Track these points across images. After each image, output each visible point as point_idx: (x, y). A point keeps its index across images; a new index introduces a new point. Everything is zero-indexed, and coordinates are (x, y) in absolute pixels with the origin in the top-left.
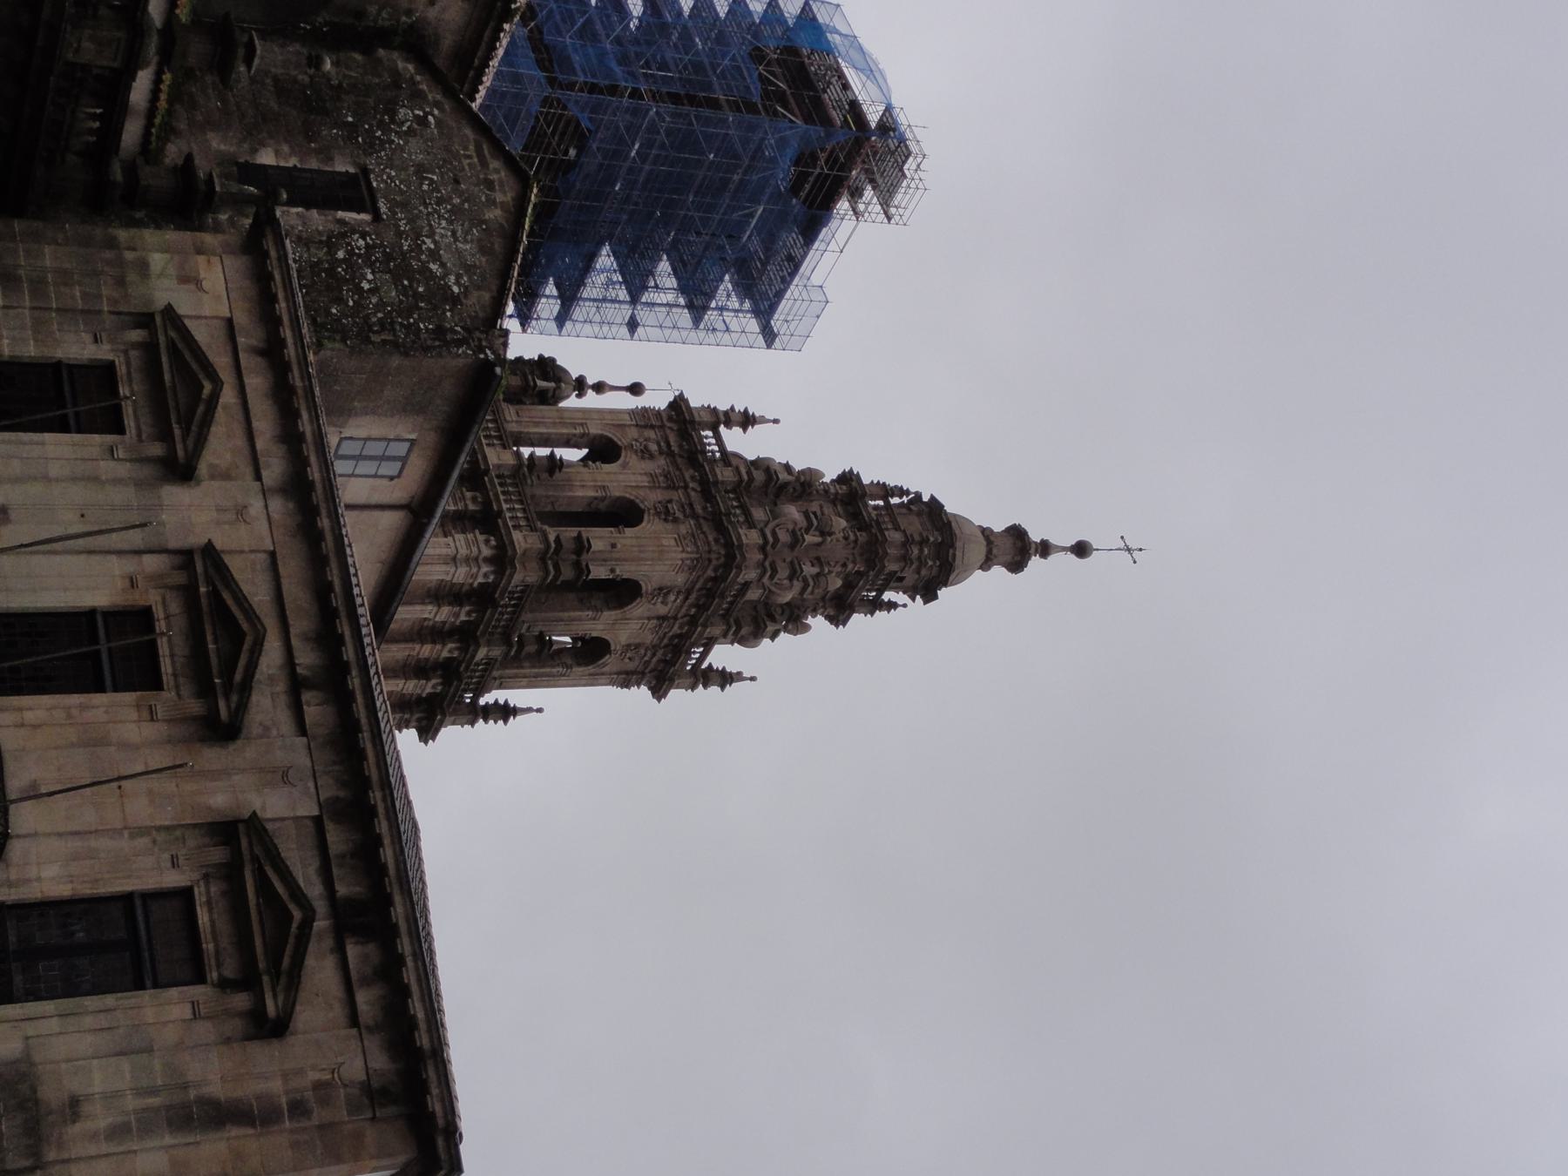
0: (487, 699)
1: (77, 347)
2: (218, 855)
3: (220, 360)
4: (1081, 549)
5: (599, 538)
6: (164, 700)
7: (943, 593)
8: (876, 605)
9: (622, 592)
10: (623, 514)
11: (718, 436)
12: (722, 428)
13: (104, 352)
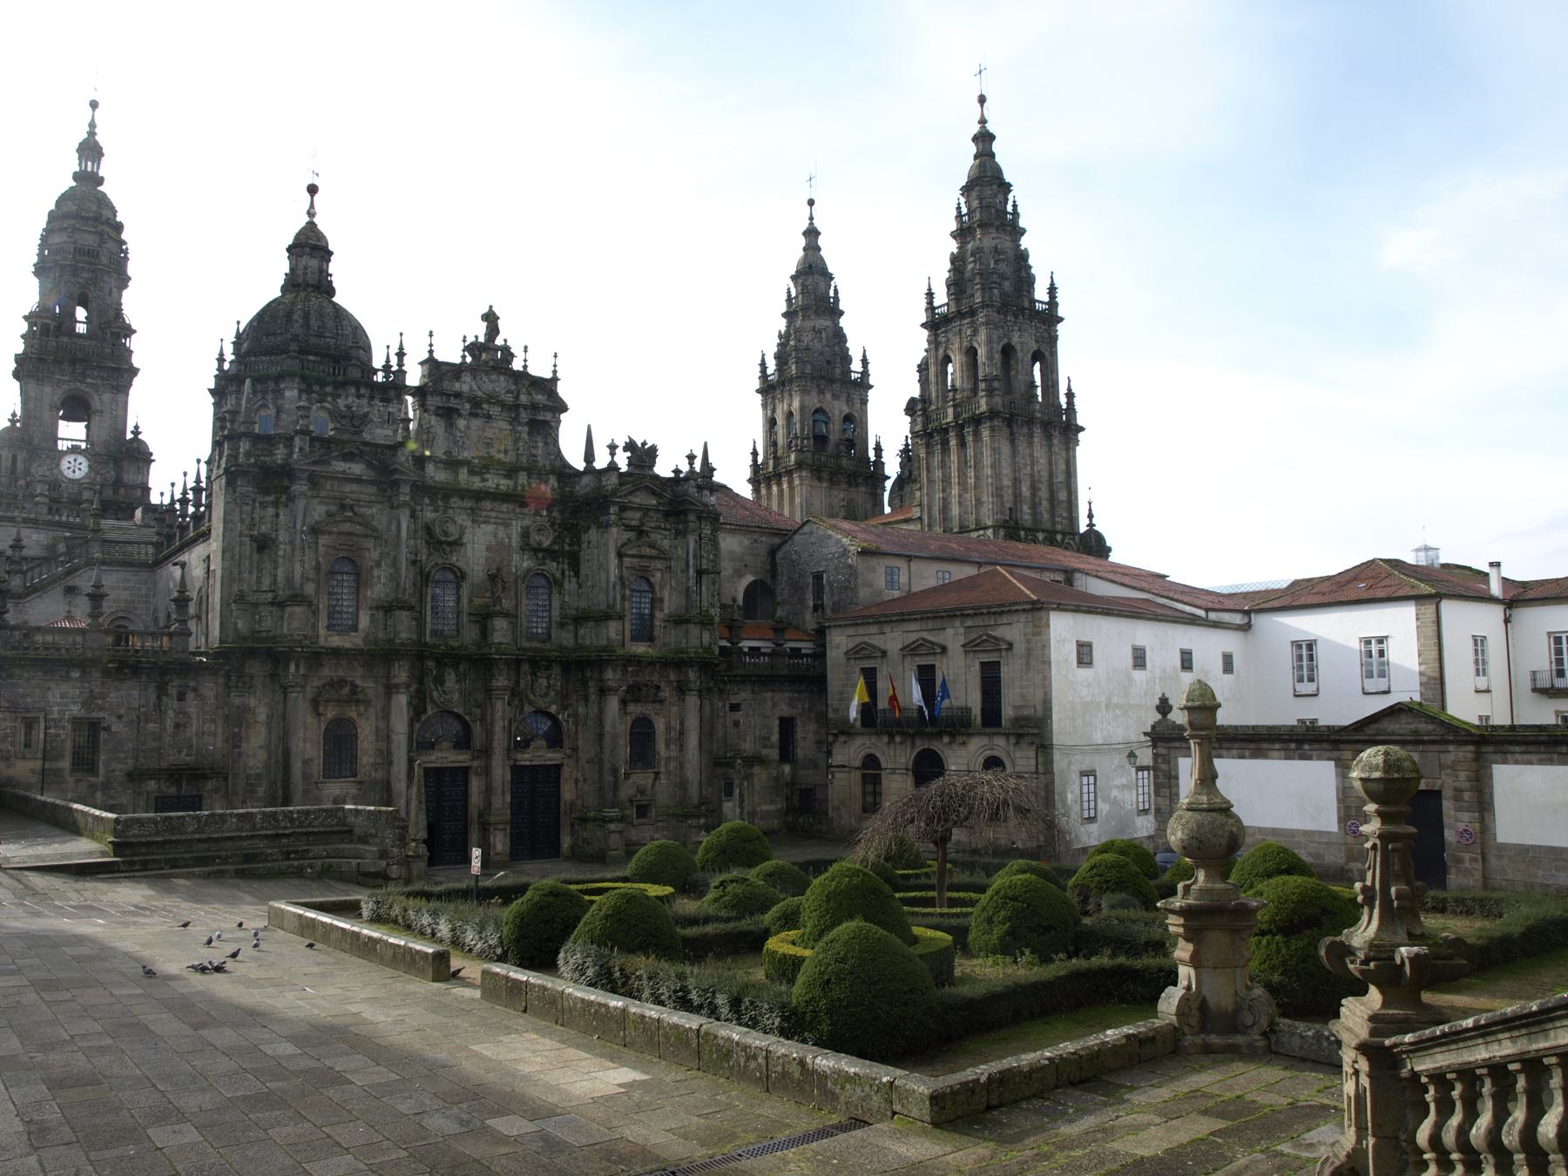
0: (1063, 400)
3: (858, 640)
5: (981, 375)
6: (938, 665)
7: (1008, 178)
8: (1015, 213)
9: (1008, 351)
10: (971, 353)
11: (938, 308)
13: (858, 670)
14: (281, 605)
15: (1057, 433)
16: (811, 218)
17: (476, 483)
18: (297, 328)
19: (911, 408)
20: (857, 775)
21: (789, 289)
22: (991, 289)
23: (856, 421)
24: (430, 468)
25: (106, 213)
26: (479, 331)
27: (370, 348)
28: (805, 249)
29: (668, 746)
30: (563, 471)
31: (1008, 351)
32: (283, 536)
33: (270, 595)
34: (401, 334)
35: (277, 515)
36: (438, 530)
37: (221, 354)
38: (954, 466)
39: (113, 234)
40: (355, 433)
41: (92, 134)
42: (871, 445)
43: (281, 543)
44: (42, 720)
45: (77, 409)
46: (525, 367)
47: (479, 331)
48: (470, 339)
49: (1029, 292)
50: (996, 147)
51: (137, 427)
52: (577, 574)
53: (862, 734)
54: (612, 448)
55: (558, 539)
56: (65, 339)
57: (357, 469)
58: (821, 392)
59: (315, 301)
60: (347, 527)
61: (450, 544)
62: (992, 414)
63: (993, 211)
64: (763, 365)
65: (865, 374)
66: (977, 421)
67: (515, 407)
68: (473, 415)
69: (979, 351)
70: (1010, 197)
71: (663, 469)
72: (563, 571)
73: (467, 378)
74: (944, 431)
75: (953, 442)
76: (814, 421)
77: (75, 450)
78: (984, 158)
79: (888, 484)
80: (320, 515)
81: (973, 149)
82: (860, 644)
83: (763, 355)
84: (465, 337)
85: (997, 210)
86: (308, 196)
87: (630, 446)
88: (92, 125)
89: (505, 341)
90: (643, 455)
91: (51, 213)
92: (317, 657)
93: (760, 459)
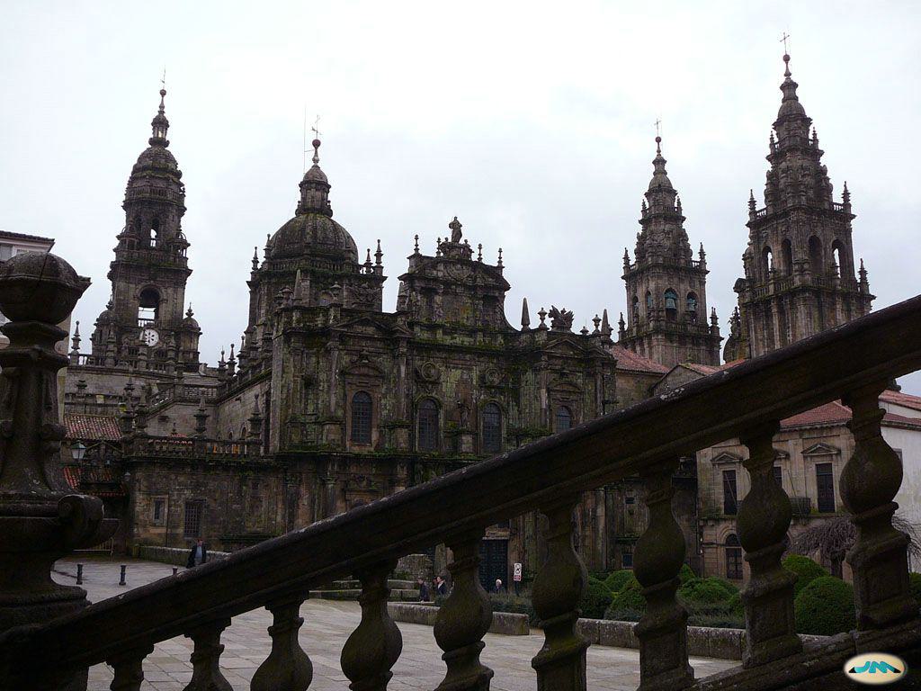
0: (858, 276)
1: (720, 478)
2: (809, 459)
4: (787, 59)
7: (808, 114)
8: (815, 140)
10: (786, 246)
12: (757, 209)
13: (721, 473)
14: (322, 424)
15: (854, 301)
16: (659, 151)
17: (448, 341)
18: (309, 239)
19: (739, 286)
20: (722, 551)
21: (644, 203)
22: (799, 196)
23: (697, 297)
24: (417, 329)
25: (171, 165)
26: (448, 234)
27: (356, 251)
28: (655, 174)
29: (583, 528)
30: (506, 329)
31: (814, 244)
32: (323, 376)
33: (313, 417)
34: (379, 241)
35: (318, 363)
36: (423, 373)
37: (256, 258)
38: (776, 328)
39: (175, 179)
40: (369, 306)
41: (162, 112)
42: (709, 314)
43: (321, 381)
44: (167, 500)
45: (150, 299)
46: (480, 259)
47: (448, 234)
48: (443, 240)
49: (828, 197)
50: (798, 92)
51: (190, 311)
52: (518, 404)
53: (725, 520)
54: (542, 314)
55: (505, 380)
56: (144, 252)
57: (370, 330)
58: (671, 277)
59: (320, 219)
60: (365, 370)
61: (431, 383)
62: (804, 289)
63: (798, 139)
64: (626, 258)
65: (703, 262)
66: (793, 293)
67: (474, 288)
68: (445, 293)
69: (792, 243)
70: (811, 128)
71: (576, 329)
72: (508, 403)
73: (441, 267)
74: (767, 302)
75: (774, 310)
76: (666, 298)
77: (148, 327)
78: (789, 102)
79: (723, 344)
80: (346, 362)
81: (781, 95)
82: (723, 453)
83: (627, 251)
84: (439, 239)
85: (801, 139)
86: (313, 148)
87: (554, 313)
88: (162, 107)
89: (466, 241)
90: (563, 319)
91: (135, 166)
92: (347, 460)
93: (626, 327)
